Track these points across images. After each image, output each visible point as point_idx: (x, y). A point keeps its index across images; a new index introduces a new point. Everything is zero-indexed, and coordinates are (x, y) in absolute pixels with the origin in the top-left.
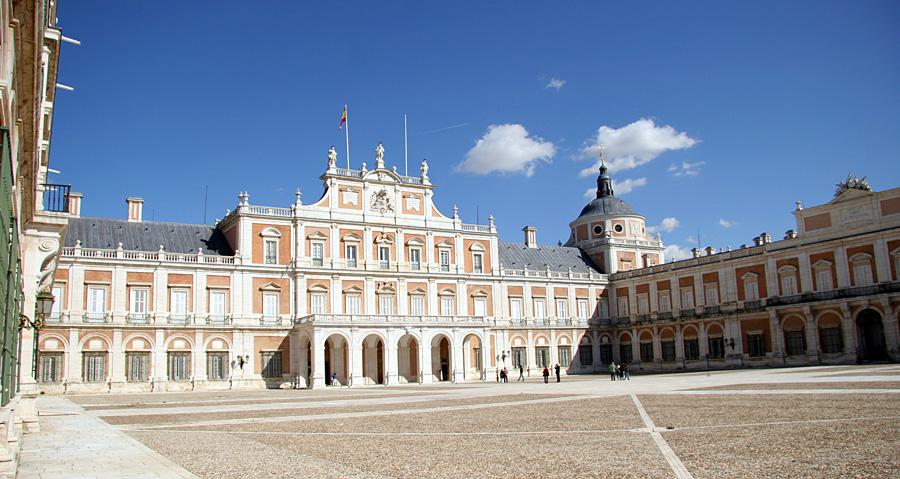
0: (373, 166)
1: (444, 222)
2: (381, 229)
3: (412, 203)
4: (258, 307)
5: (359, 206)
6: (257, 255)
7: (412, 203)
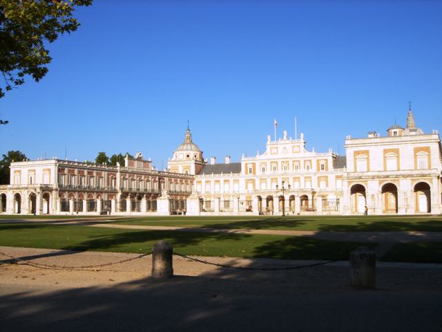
0: (282, 138)
1: (308, 154)
2: (283, 160)
3: (296, 149)
4: (247, 187)
5: (277, 153)
6: (246, 173)
7: (296, 149)
